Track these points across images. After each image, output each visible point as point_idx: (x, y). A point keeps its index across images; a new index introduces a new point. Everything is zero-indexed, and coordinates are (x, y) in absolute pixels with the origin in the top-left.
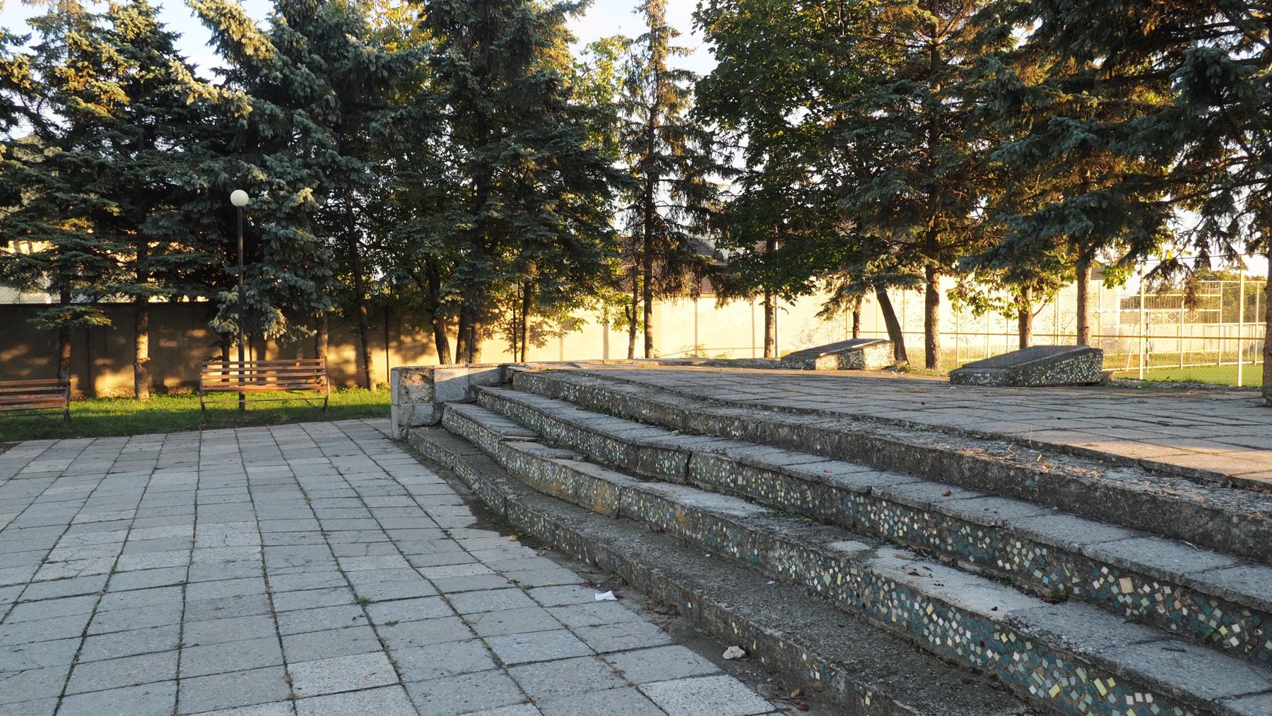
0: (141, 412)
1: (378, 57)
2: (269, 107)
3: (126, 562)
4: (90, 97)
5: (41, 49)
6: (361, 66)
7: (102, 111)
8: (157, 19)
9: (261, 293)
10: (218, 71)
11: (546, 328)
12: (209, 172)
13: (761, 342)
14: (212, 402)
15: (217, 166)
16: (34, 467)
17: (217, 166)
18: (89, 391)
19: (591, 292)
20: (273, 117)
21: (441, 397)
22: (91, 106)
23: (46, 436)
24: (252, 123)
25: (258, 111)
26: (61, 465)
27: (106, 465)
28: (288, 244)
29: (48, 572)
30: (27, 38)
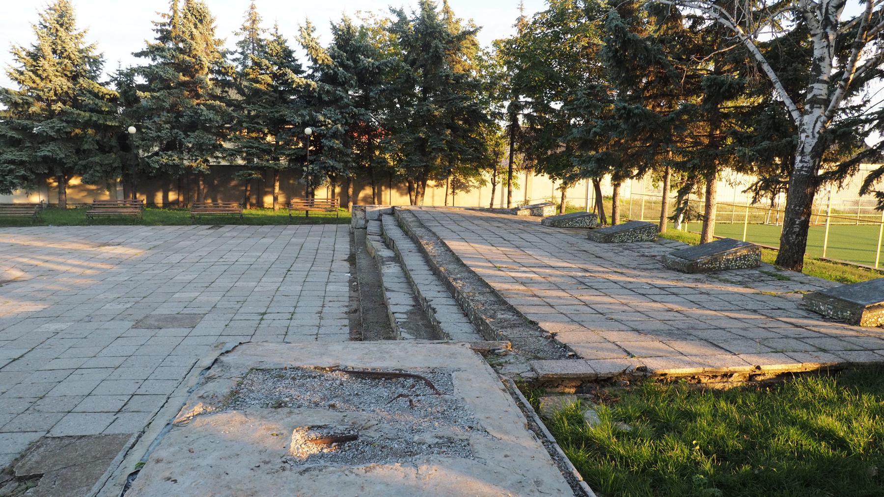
0: (271, 217)
1: (373, 64)
2: (327, 87)
3: (240, 259)
4: (257, 82)
5: (242, 53)
6: (366, 69)
7: (262, 87)
8: (286, 44)
9: (321, 168)
10: (310, 68)
11: (470, 183)
12: (302, 115)
13: (506, 201)
14: (294, 213)
15: (305, 113)
16: (227, 234)
17: (305, 113)
18: (260, 205)
19: (484, 168)
20: (328, 92)
21: (368, 218)
22: (258, 85)
23: (234, 224)
24: (319, 94)
25: (322, 88)
26: (235, 234)
27: (249, 235)
28: (331, 148)
29: (221, 260)
30: (236, 52)
